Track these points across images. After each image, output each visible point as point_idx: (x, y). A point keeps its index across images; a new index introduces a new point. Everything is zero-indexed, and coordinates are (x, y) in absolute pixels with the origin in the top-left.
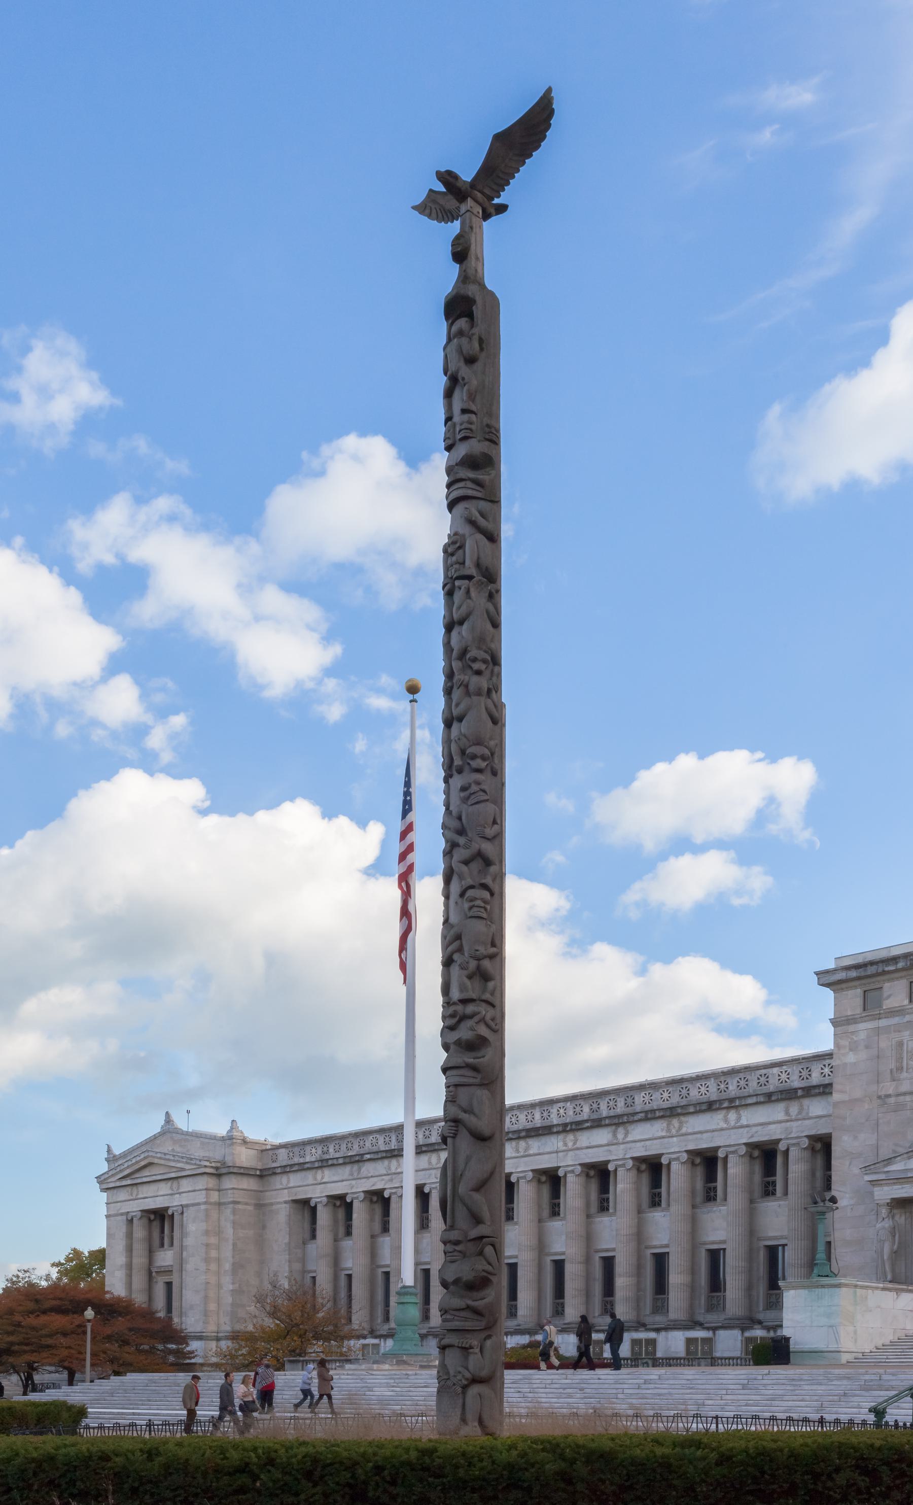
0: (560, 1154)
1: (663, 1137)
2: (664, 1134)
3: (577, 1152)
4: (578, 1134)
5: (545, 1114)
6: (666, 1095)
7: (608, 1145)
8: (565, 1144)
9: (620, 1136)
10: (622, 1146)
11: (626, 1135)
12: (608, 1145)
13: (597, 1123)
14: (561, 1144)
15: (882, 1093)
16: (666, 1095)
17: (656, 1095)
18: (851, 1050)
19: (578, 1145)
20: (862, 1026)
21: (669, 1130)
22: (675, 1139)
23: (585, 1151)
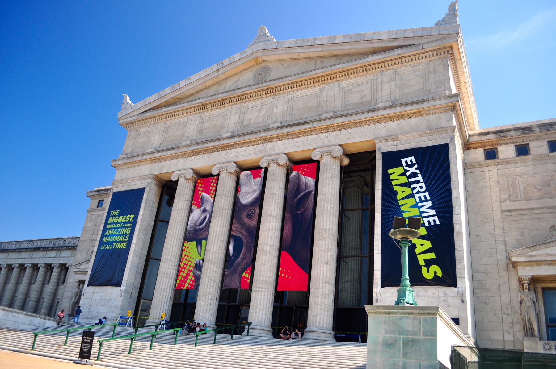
0: (41, 259)
1: (69, 257)
2: (70, 255)
3: (45, 259)
4: (48, 252)
5: (41, 243)
6: (75, 241)
7: (54, 257)
8: (43, 255)
9: (58, 254)
10: (58, 258)
11: (60, 254)
12: (54, 257)
13: (53, 249)
14: (42, 255)
15: (93, 239)
16: (75, 241)
17: (72, 241)
18: (90, 221)
19: (46, 256)
20: (96, 213)
21: (72, 254)
22: (72, 258)
23: (47, 259)
